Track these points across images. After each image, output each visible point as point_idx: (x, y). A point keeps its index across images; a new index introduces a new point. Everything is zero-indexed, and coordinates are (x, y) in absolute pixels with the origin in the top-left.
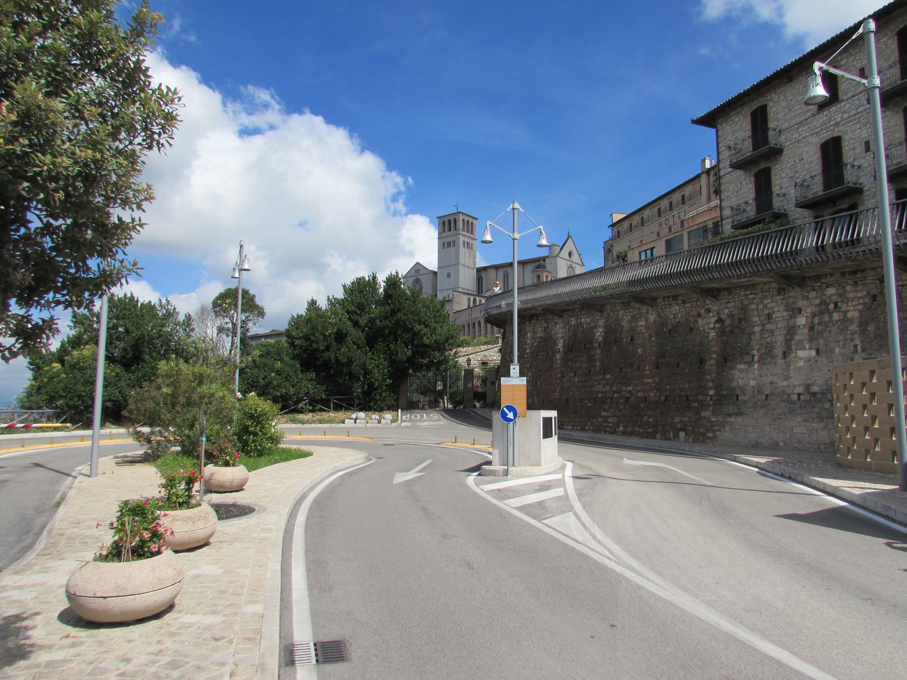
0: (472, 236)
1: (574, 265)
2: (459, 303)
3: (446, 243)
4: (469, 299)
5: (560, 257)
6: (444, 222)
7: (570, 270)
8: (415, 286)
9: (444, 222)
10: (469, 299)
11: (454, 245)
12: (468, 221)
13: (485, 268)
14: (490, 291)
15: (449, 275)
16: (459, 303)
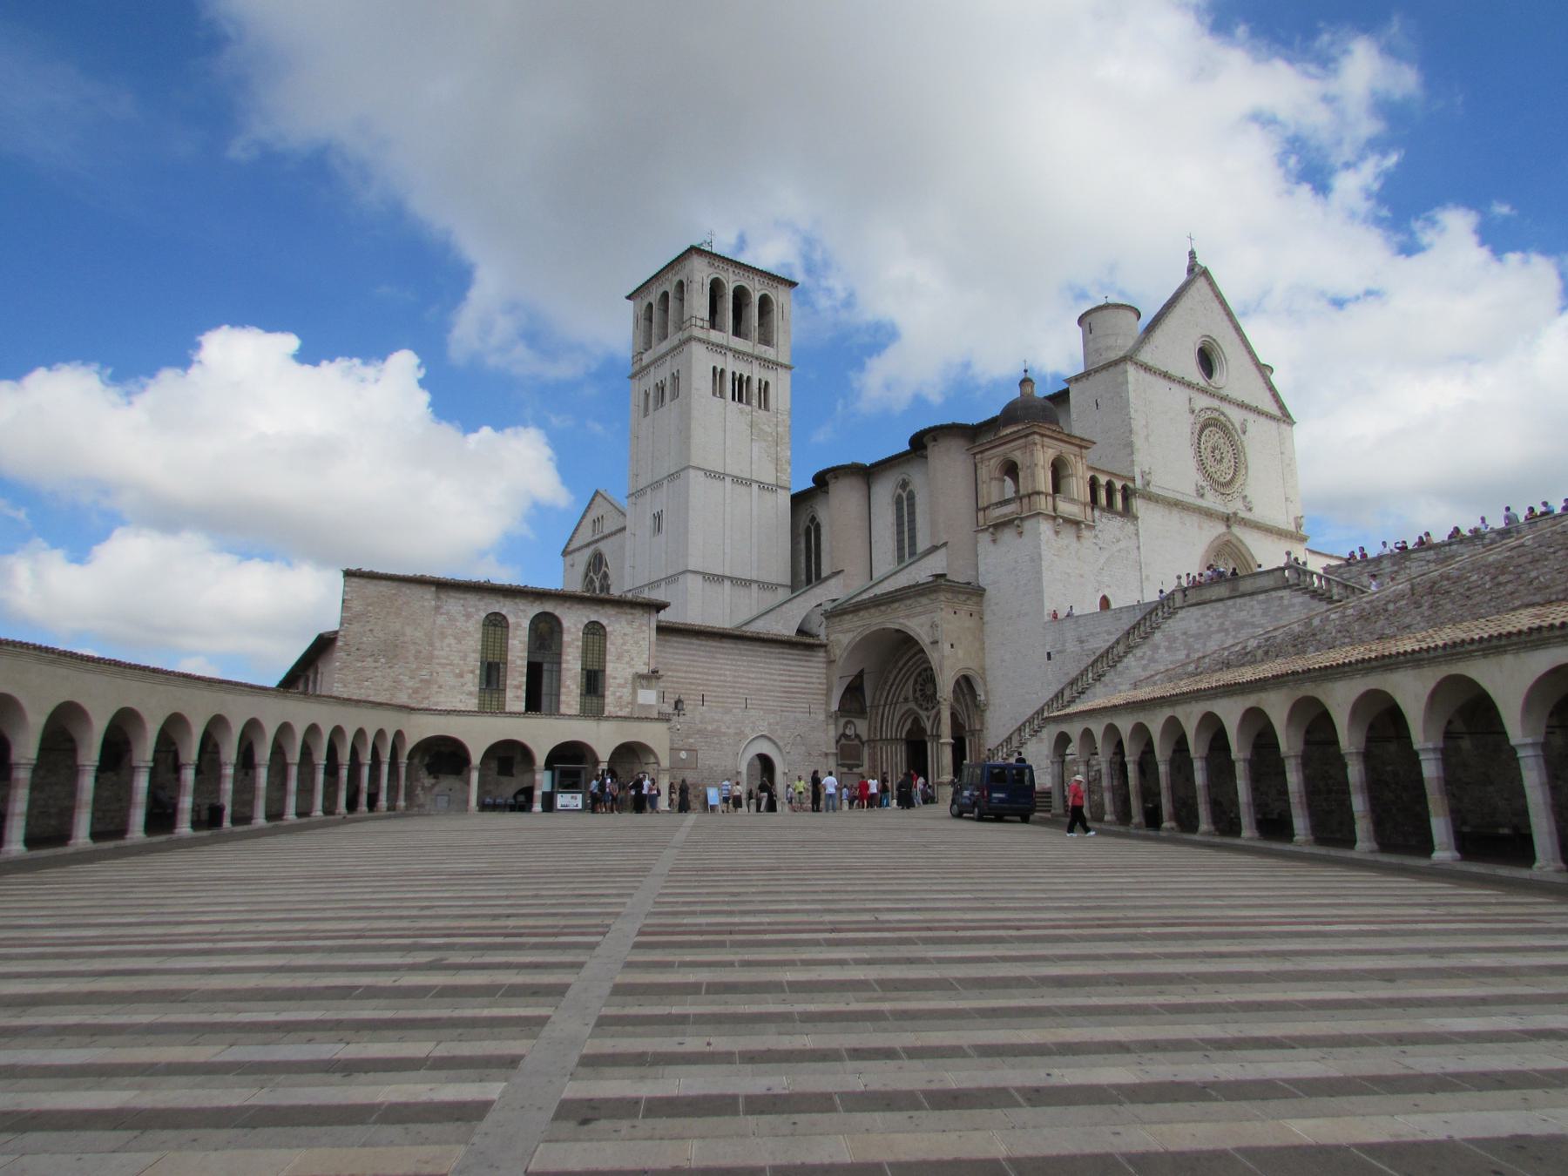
0: (769, 353)
1: (1235, 415)
2: (391, 651)
3: (652, 394)
4: (496, 622)
5: (1147, 368)
6: (650, 306)
7: (1213, 437)
8: (592, 581)
9: (650, 306)
10: (496, 622)
11: (675, 395)
12: (740, 295)
13: (822, 481)
14: (833, 582)
15: (658, 518)
16: (391, 651)
